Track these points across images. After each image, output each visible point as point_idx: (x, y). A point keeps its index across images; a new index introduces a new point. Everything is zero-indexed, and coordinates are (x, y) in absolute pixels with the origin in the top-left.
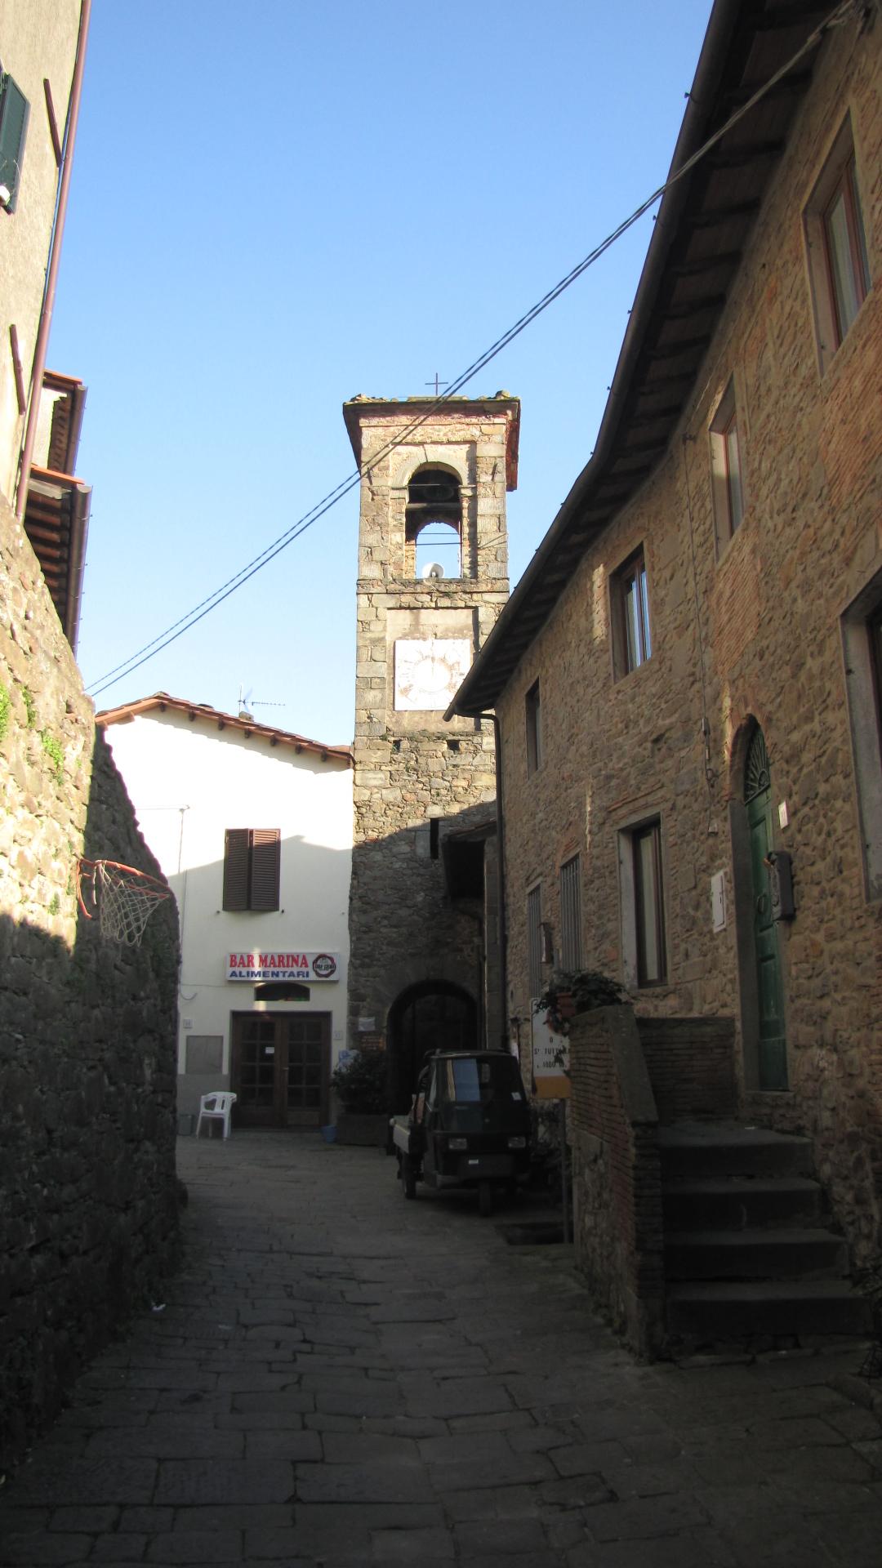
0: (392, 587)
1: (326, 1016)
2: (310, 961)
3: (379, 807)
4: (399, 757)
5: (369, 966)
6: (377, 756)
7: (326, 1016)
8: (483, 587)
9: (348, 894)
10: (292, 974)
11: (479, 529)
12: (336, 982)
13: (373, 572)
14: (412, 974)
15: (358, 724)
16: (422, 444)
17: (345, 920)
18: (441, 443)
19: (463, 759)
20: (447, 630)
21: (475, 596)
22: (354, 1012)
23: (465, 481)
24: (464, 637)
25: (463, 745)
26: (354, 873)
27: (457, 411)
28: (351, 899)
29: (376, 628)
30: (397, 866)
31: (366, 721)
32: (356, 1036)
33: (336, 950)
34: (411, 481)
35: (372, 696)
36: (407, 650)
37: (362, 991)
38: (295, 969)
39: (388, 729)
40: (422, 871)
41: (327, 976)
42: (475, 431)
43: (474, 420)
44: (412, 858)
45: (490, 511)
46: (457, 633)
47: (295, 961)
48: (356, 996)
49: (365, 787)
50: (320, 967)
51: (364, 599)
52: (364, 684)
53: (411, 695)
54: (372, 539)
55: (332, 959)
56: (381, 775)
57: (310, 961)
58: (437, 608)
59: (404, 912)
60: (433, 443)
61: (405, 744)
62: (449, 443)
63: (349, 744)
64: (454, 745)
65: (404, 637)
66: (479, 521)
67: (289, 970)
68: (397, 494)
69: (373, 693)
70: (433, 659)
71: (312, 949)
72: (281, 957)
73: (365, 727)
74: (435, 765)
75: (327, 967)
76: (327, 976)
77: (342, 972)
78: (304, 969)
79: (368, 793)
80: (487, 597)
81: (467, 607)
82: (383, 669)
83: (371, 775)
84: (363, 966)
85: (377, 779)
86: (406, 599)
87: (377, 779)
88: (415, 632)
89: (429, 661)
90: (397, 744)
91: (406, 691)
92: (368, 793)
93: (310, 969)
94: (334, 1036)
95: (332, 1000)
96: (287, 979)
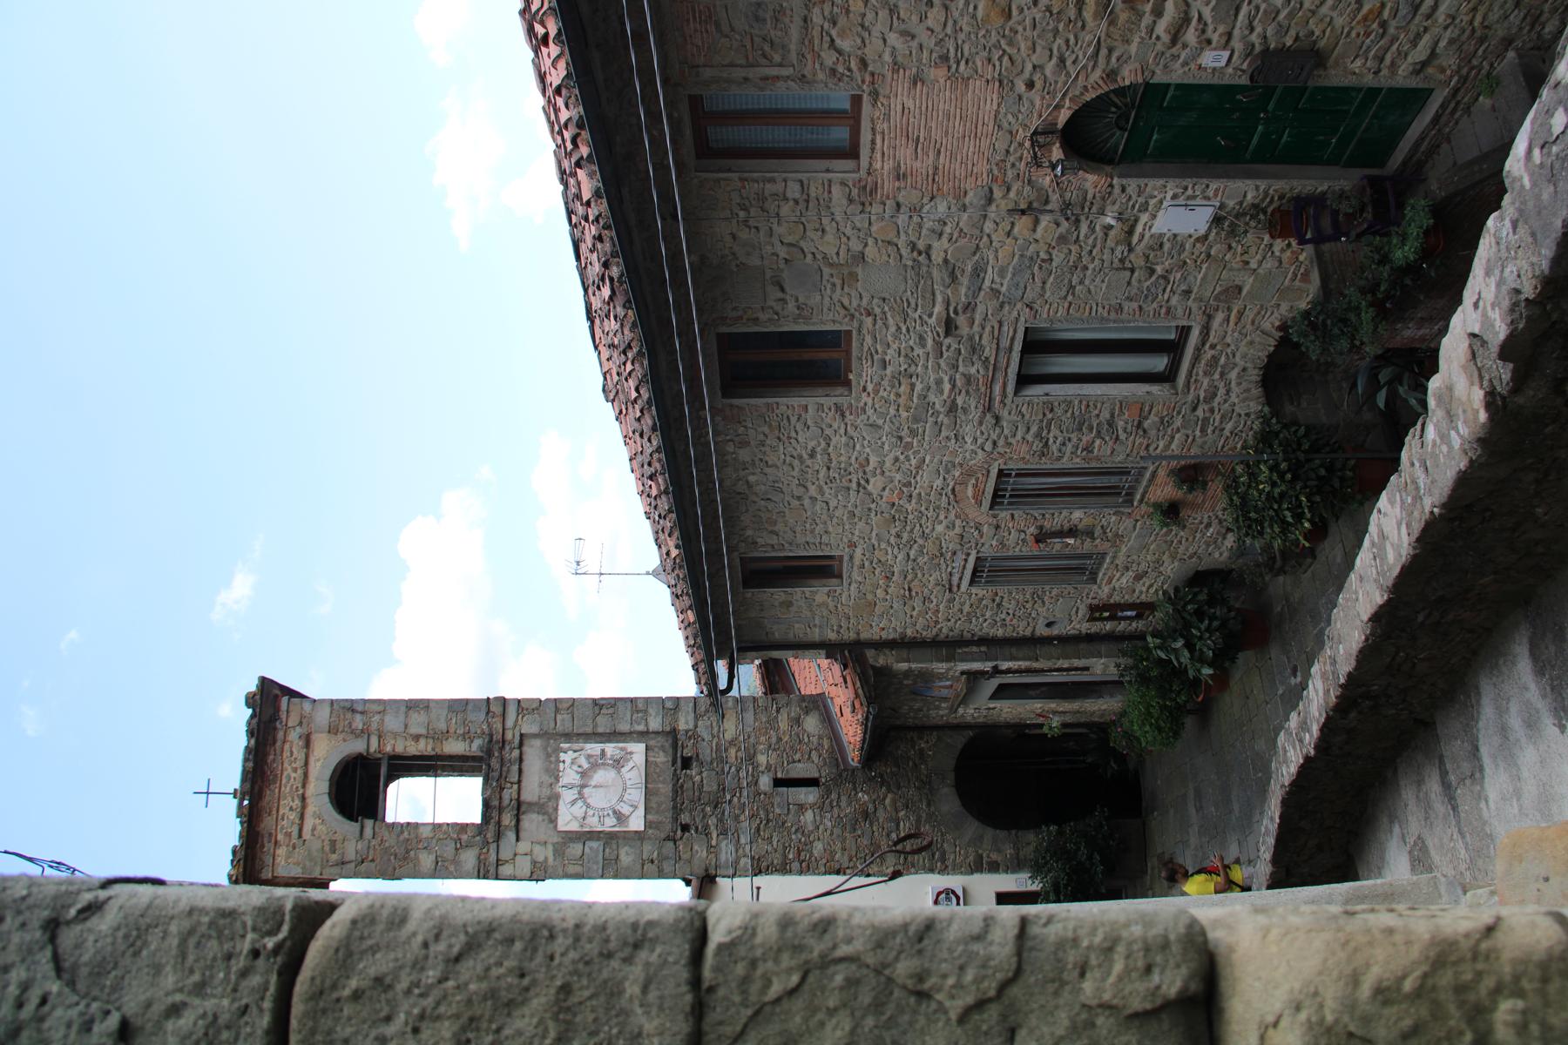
0: (490, 836)
8: (499, 726)
11: (423, 731)
14: (949, 801)
16: (303, 798)
18: (306, 775)
19: (706, 753)
20: (547, 770)
21: (509, 736)
22: (994, 868)
23: (357, 746)
24: (558, 750)
25: (688, 753)
27: (266, 755)
29: (541, 853)
32: (1015, 866)
35: (626, 856)
36: (569, 818)
39: (668, 839)
41: (958, 898)
42: (294, 736)
43: (280, 734)
44: (820, 807)
45: (402, 718)
48: (977, 867)
49: (737, 862)
51: (506, 869)
53: (625, 810)
54: (427, 860)
55: (939, 894)
56: (723, 844)
58: (519, 782)
59: (881, 814)
60: (304, 786)
61: (685, 818)
62: (306, 764)
64: (686, 763)
65: (553, 821)
66: (414, 730)
68: (368, 831)
70: (583, 786)
74: (710, 786)
76: (958, 898)
77: (955, 881)
80: (510, 723)
81: (521, 744)
83: (723, 857)
84: (943, 859)
85: (726, 851)
86: (507, 819)
87: (726, 851)
88: (547, 808)
89: (586, 790)
90: (685, 828)
91: (620, 818)
92: (743, 861)
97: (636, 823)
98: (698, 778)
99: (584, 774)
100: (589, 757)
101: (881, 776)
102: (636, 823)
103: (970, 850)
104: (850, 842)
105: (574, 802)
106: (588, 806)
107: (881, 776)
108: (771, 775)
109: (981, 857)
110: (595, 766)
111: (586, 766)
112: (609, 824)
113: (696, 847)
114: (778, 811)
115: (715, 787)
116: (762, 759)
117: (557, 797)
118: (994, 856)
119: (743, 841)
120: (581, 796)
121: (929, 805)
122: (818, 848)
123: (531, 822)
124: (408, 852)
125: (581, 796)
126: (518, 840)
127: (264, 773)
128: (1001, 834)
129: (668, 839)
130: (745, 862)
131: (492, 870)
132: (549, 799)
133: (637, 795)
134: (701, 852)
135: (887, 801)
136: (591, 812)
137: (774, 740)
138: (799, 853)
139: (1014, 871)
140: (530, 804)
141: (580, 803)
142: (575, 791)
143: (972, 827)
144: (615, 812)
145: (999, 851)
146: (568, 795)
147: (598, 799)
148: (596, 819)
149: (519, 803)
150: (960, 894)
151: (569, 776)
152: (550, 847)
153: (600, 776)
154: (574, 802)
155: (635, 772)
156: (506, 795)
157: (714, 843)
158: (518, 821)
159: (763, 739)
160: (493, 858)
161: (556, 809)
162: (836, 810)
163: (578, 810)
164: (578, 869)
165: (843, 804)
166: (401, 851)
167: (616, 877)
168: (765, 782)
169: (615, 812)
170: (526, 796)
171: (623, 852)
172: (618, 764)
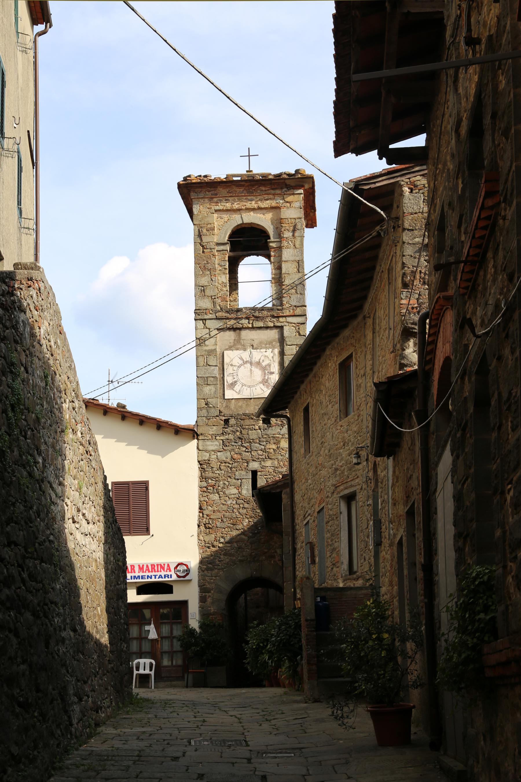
0: (219, 314)
1: (184, 604)
2: (172, 568)
3: (215, 464)
4: (229, 430)
5: (211, 569)
6: (213, 430)
7: (184, 604)
9: (196, 522)
10: (160, 576)
12: (190, 580)
13: (207, 304)
14: (241, 573)
15: (199, 409)
17: (195, 540)
20: (261, 343)
22: (202, 600)
26: (200, 508)
27: (264, 185)
28: (199, 526)
30: (229, 502)
31: (204, 405)
33: (189, 560)
34: (231, 236)
35: (207, 390)
36: (232, 357)
37: (208, 586)
38: (163, 573)
39: (220, 412)
40: (246, 505)
46: (268, 344)
47: (162, 568)
49: (206, 451)
50: (179, 571)
51: (200, 324)
52: (202, 381)
53: (237, 388)
54: (204, 281)
57: (172, 568)
58: (253, 328)
61: (232, 421)
63: (194, 423)
65: (230, 348)
67: (158, 574)
69: (208, 388)
70: (251, 363)
71: (173, 560)
72: (153, 566)
73: (204, 411)
74: (253, 435)
75: (184, 571)
77: (194, 576)
78: (169, 573)
79: (208, 454)
82: (216, 371)
83: (209, 443)
84: (208, 569)
85: (213, 445)
87: (213, 445)
89: (248, 365)
90: (226, 422)
91: (233, 385)
92: (208, 454)
93: (172, 573)
94: (190, 616)
95: (189, 594)
96: (157, 580)
97: (229, 394)
98: (257, 427)
99: (258, 363)
100: (269, 365)
101: (258, 533)
102: (229, 394)
103: (213, 586)
104: (219, 515)
105: (241, 358)
106: (239, 367)
107: (258, 533)
108: (260, 469)
109: (209, 592)
110: (264, 369)
111: (264, 364)
112: (228, 379)
113: (215, 428)
114: (237, 473)
115: (251, 438)
116: (269, 463)
117: (245, 350)
118: (209, 600)
119: (219, 454)
120: (245, 363)
121: (241, 561)
122: (216, 497)
123: (230, 335)
124: (210, 270)
125: (246, 362)
126: (218, 329)
127: (253, 186)
128: (223, 604)
129: (220, 412)
130: (206, 456)
131: (200, 317)
132: (244, 345)
133: (246, 393)
134: (213, 430)
135: (243, 536)
136: (235, 368)
137: (280, 470)
138: (213, 486)
139: (200, 611)
140: (239, 335)
141: (241, 362)
142: (248, 359)
143: (227, 587)
144: (236, 382)
145: (213, 603)
146: (245, 355)
147: (243, 373)
148: (232, 372)
149: (240, 329)
150: (187, 578)
151: (257, 355)
152: (213, 348)
153: (258, 374)
154: (241, 358)
155: (261, 392)
156: (245, 322)
157: (218, 438)
158: (229, 329)
159: (282, 463)
160: (206, 317)
161: (237, 349)
162: (237, 506)
163: (237, 362)
164: (202, 364)
165: (241, 511)
166: (209, 266)
167: (198, 384)
168: (254, 465)
169: (236, 382)
170: (244, 333)
171: (212, 388)
172: (265, 382)
